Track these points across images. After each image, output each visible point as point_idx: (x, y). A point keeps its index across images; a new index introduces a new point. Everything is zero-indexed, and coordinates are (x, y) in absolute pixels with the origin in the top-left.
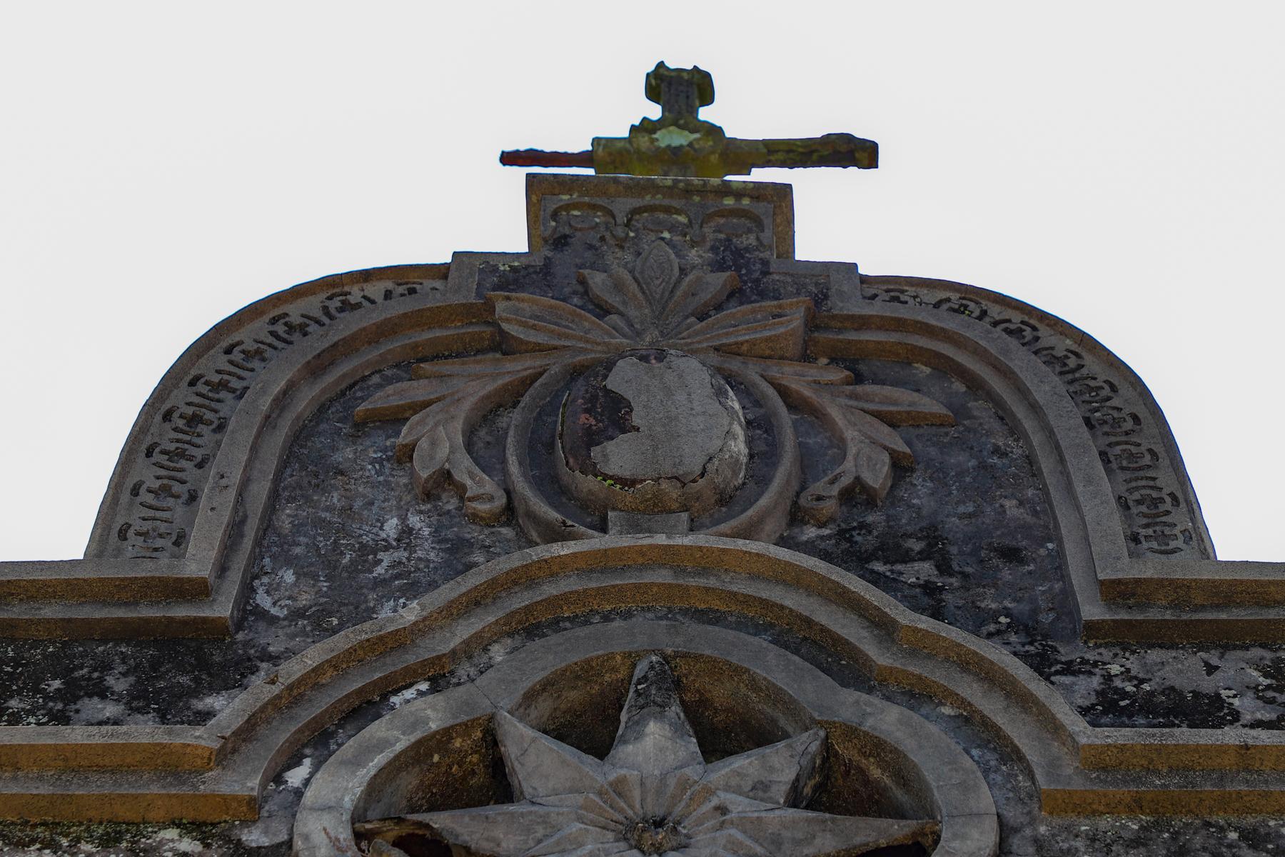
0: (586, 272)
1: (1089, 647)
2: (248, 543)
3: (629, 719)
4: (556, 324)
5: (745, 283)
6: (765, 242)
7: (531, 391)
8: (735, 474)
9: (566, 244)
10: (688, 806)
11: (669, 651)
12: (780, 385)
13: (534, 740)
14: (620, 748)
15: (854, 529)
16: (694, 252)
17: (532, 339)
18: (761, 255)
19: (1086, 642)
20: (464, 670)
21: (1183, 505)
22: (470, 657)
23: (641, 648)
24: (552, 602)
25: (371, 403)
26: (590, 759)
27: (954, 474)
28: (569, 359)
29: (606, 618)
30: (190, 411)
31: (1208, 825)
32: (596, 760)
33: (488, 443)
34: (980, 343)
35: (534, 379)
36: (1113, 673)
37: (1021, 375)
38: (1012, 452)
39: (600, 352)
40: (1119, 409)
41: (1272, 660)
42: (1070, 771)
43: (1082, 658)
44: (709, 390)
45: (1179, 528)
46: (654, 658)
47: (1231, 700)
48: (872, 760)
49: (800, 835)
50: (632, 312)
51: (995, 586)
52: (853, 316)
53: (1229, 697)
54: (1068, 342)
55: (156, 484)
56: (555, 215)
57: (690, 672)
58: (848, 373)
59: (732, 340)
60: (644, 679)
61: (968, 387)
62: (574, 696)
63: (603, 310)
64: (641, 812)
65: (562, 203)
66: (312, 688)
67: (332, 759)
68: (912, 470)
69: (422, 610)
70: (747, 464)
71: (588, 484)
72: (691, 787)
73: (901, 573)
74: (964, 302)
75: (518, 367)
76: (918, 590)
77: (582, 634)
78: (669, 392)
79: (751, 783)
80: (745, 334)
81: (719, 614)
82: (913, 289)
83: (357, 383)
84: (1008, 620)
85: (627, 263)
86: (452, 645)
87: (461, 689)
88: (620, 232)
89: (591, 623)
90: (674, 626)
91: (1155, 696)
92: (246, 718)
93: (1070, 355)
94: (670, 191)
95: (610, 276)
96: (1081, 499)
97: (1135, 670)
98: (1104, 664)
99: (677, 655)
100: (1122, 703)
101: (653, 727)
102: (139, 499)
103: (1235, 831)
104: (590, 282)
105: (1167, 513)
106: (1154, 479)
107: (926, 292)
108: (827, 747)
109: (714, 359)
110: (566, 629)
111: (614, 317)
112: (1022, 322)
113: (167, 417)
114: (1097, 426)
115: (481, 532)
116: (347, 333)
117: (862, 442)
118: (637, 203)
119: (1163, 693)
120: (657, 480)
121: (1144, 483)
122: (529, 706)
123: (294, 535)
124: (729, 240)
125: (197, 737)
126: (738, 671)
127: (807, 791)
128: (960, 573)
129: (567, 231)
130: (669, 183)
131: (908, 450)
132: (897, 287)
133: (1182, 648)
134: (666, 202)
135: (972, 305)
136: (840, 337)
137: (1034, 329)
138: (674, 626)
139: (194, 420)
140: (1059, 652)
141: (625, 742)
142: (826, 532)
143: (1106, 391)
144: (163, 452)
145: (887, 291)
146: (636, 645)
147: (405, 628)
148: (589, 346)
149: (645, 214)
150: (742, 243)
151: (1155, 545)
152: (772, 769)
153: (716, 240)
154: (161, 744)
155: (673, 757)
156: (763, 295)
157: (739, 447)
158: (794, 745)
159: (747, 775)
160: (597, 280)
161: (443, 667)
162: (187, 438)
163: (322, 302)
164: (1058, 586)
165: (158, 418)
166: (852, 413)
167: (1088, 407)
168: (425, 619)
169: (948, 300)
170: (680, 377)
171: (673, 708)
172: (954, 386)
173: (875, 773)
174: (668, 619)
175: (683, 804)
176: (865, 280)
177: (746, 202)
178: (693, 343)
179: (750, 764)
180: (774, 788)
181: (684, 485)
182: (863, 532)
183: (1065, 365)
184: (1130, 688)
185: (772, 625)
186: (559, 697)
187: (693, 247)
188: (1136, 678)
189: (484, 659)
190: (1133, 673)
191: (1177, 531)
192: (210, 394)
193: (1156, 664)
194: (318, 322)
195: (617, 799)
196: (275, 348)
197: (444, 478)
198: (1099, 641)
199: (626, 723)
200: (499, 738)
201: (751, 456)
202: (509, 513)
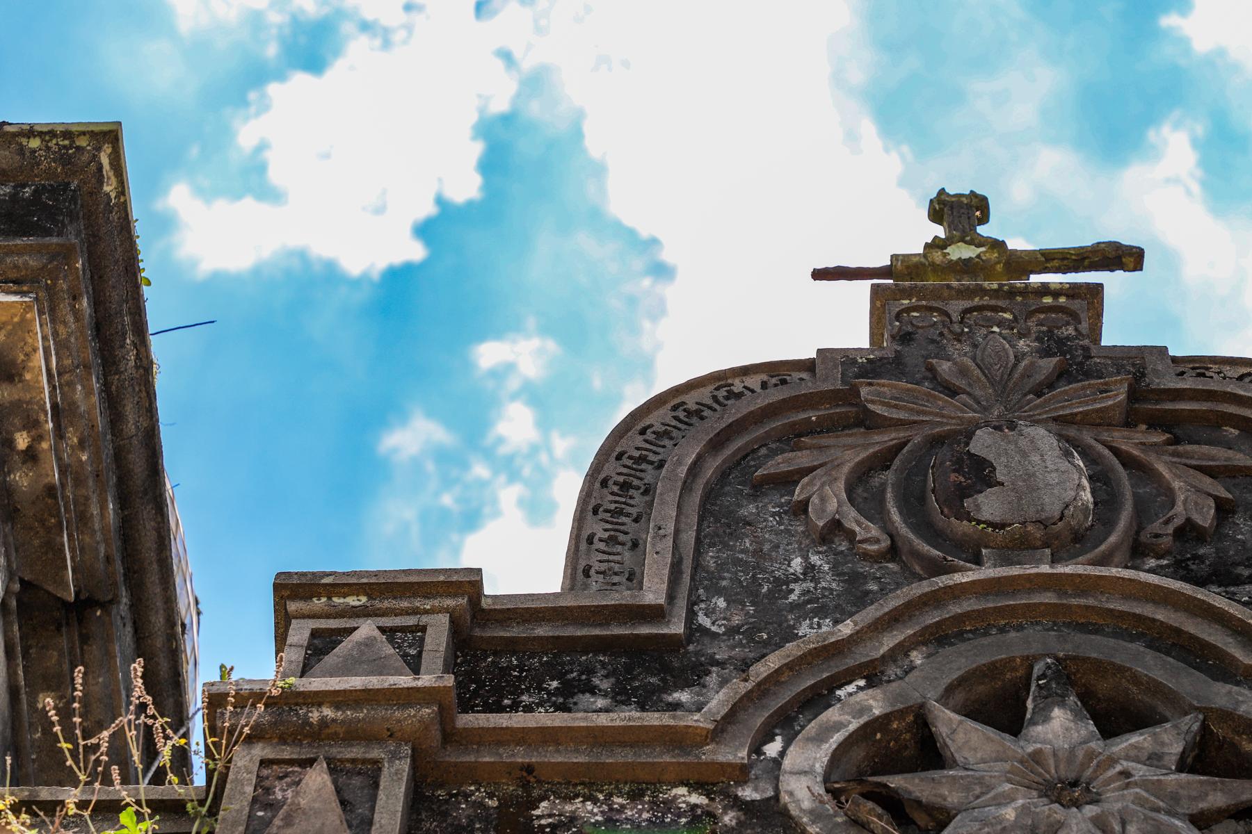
2: (686, 578)
3: (1035, 706)
4: (913, 403)
5: (1071, 365)
6: (1084, 332)
7: (900, 457)
8: (1086, 518)
9: (912, 339)
10: (1095, 771)
11: (1061, 654)
13: (961, 722)
14: (1031, 729)
15: (1189, 559)
16: (1022, 342)
20: (892, 671)
22: (895, 661)
23: (1037, 653)
24: (959, 619)
25: (765, 469)
28: (928, 431)
29: (1002, 630)
30: (621, 479)
35: (905, 444)
39: (954, 424)
44: (1057, 452)
46: (1049, 660)
49: (1194, 794)
50: (978, 392)
52: (1169, 390)
55: (606, 535)
56: (898, 317)
57: (1078, 671)
58: (1168, 436)
59: (1068, 411)
60: (1043, 676)
62: (981, 689)
63: (953, 392)
64: (1056, 776)
65: (903, 307)
66: (775, 685)
67: (800, 736)
68: (1234, 512)
69: (855, 625)
70: (1094, 510)
71: (964, 527)
72: (1097, 757)
77: (986, 642)
78: (1024, 455)
79: (1146, 754)
80: (1078, 407)
81: (1097, 626)
83: (747, 454)
86: (882, 652)
87: (894, 684)
88: (957, 328)
89: (991, 635)
90: (1062, 636)
92: (730, 707)
94: (996, 294)
99: (1067, 658)
101: (1057, 712)
102: (594, 547)
107: (1228, 368)
110: (969, 639)
113: (604, 483)
115: (871, 567)
116: (739, 415)
117: (1189, 491)
118: (967, 304)
120: (1023, 523)
122: (948, 698)
123: (719, 572)
124: (1050, 331)
125: (696, 721)
126: (1121, 669)
127: (1189, 760)
129: (910, 329)
130: (995, 286)
131: (1230, 496)
132: (1202, 365)
134: (993, 302)
136: (1158, 407)
139: (625, 486)
141: (1033, 723)
144: (606, 511)
145: (1193, 368)
146: (1032, 651)
147: (843, 639)
148: (945, 420)
149: (975, 313)
150: (1063, 333)
152: (1163, 744)
153: (1040, 332)
154: (669, 726)
155: (1077, 734)
156: (1088, 375)
158: (1179, 726)
160: (944, 367)
161: (875, 668)
162: (623, 500)
163: (711, 392)
165: (597, 485)
166: (1177, 468)
168: (858, 632)
170: (1032, 442)
171: (1071, 698)
175: (1091, 770)
177: (1062, 300)
178: (1034, 415)
179: (1145, 739)
180: (1167, 758)
181: (1046, 527)
182: (1196, 562)
185: (1143, 634)
186: (970, 690)
187: (1021, 338)
189: (907, 662)
192: (634, 466)
194: (710, 408)
195: (1036, 766)
196: (679, 429)
197: (836, 526)
199: (1033, 709)
200: (929, 721)
201: (1096, 504)
202: (893, 552)
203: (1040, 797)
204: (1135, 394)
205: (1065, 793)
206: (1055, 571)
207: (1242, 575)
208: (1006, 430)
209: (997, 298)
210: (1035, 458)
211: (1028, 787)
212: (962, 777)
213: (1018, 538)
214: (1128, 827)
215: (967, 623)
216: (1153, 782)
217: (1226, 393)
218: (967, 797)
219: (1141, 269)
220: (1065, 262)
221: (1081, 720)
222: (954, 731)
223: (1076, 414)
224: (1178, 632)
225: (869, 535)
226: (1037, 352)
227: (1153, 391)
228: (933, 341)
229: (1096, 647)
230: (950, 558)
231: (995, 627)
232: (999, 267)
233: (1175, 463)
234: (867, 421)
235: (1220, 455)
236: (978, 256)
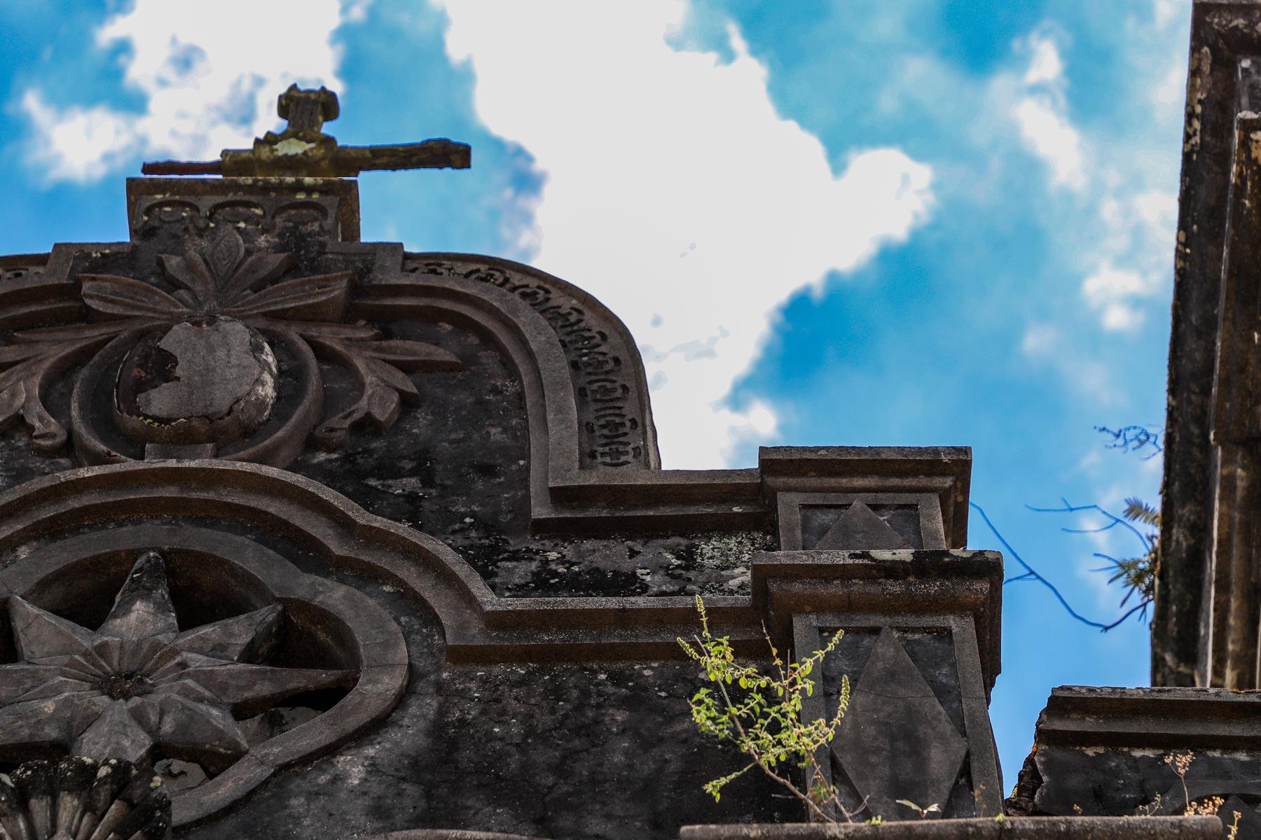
0: (164, 256)
3: (122, 600)
4: (131, 299)
6: (326, 228)
7: (102, 352)
8: (261, 412)
9: (154, 234)
10: (156, 663)
12: (317, 342)
15: (359, 453)
16: (263, 238)
17: (109, 311)
18: (321, 239)
19: (533, 536)
21: (640, 428)
26: (84, 630)
27: (453, 408)
28: (137, 326)
32: (89, 631)
33: (62, 394)
34: (495, 304)
36: (550, 558)
37: (522, 329)
38: (507, 390)
39: (165, 320)
40: (604, 354)
41: (687, 546)
42: (475, 631)
43: (527, 548)
44: (247, 347)
45: (632, 446)
47: (644, 577)
48: (319, 627)
50: (198, 288)
51: (468, 495)
53: (642, 575)
54: (574, 302)
56: (148, 211)
59: (279, 307)
61: (481, 340)
63: (173, 284)
65: (154, 202)
68: (418, 406)
70: (273, 405)
71: (133, 422)
73: (390, 486)
74: (491, 272)
75: (94, 334)
76: (401, 499)
78: (211, 349)
82: (450, 263)
84: (472, 520)
85: (202, 249)
90: (173, 530)
93: (573, 312)
94: (250, 189)
95: (185, 259)
96: (550, 425)
98: (545, 551)
99: (171, 551)
101: (139, 607)
103: (605, 673)
104: (167, 264)
105: (625, 434)
106: (620, 408)
108: (283, 618)
109: (262, 323)
111: (182, 292)
112: (539, 287)
114: (583, 368)
117: (378, 385)
119: (588, 573)
120: (188, 418)
121: (611, 411)
124: (296, 227)
126: (222, 562)
127: (263, 650)
128: (440, 485)
129: (156, 223)
130: (250, 181)
133: (613, 539)
134: (246, 198)
135: (497, 274)
136: (377, 303)
137: (547, 291)
138: (173, 530)
140: (509, 544)
141: (116, 617)
142: (335, 456)
143: (598, 339)
148: (156, 315)
149: (228, 209)
150: (307, 229)
151: (608, 460)
155: (152, 627)
156: (315, 271)
157: (267, 390)
159: (208, 640)
160: (173, 262)
166: (375, 363)
167: (579, 353)
169: (478, 271)
170: (225, 337)
172: (469, 340)
173: (322, 636)
174: (171, 524)
176: (408, 257)
177: (315, 196)
178: (245, 310)
181: (212, 421)
183: (568, 320)
184: (561, 569)
188: (568, 562)
191: (629, 448)
195: (99, 659)
199: (119, 602)
201: (278, 398)
203: (92, 689)
204: (358, 288)
205: (118, 685)
206: (180, 465)
207: (404, 468)
208: (204, 326)
209: (251, 194)
210: (221, 353)
211: (83, 680)
212: (16, 671)
213: (182, 433)
214: (165, 718)
215: (86, 518)
216: (205, 673)
217: (444, 289)
218: (16, 691)
219: (469, 167)
220: (394, 159)
221: (163, 613)
222: (28, 626)
223: (288, 310)
224: (286, 523)
225: (47, 431)
226: (273, 248)
227: (375, 287)
228: (175, 236)
229: (200, 539)
230: (114, 453)
231: (114, 521)
232: (324, 164)
233: (375, 358)
234: (88, 317)
235: (422, 350)
236: (305, 153)
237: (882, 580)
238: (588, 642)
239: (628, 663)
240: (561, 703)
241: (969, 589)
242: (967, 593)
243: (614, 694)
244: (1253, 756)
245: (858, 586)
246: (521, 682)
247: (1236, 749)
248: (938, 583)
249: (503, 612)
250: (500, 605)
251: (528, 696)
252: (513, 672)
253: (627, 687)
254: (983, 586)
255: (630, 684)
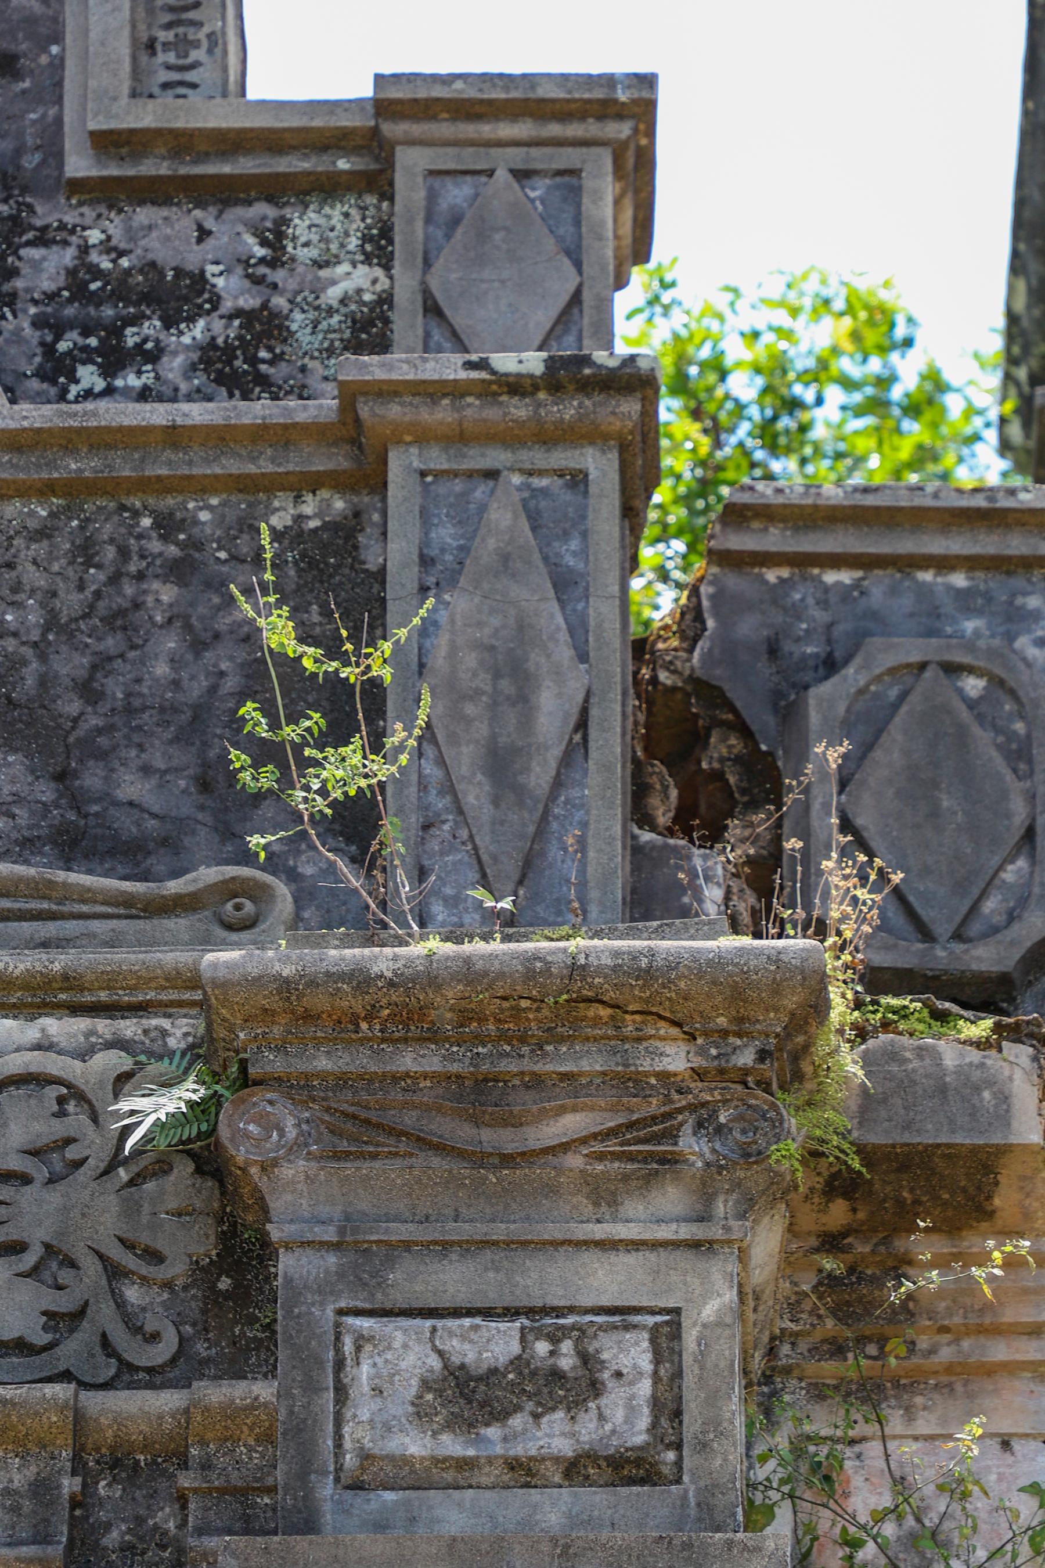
1: (70, 205)
19: (68, 199)
31: (123, 508)
36: (91, 242)
91: (131, 275)
97: (119, 239)
98: (84, 229)
100: (94, 286)
119: (141, 271)
164: (52, 112)
184: (106, 265)
188: (115, 249)
190: (114, 242)
193: (142, 228)
198: (83, 198)
237: (504, 398)
238: (126, 473)
239: (180, 499)
240: (92, 571)
241: (613, 413)
242: (611, 419)
243: (161, 554)
244: (972, 579)
245: (473, 408)
246: (43, 533)
247: (952, 568)
248: (575, 403)
249: (16, 430)
250: (12, 418)
251: (51, 557)
252: (32, 514)
253: (177, 544)
254: (631, 407)
255: (182, 537)
